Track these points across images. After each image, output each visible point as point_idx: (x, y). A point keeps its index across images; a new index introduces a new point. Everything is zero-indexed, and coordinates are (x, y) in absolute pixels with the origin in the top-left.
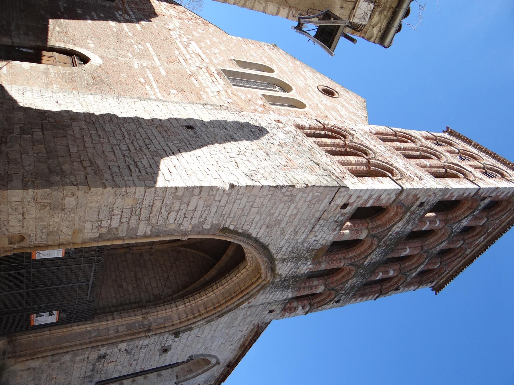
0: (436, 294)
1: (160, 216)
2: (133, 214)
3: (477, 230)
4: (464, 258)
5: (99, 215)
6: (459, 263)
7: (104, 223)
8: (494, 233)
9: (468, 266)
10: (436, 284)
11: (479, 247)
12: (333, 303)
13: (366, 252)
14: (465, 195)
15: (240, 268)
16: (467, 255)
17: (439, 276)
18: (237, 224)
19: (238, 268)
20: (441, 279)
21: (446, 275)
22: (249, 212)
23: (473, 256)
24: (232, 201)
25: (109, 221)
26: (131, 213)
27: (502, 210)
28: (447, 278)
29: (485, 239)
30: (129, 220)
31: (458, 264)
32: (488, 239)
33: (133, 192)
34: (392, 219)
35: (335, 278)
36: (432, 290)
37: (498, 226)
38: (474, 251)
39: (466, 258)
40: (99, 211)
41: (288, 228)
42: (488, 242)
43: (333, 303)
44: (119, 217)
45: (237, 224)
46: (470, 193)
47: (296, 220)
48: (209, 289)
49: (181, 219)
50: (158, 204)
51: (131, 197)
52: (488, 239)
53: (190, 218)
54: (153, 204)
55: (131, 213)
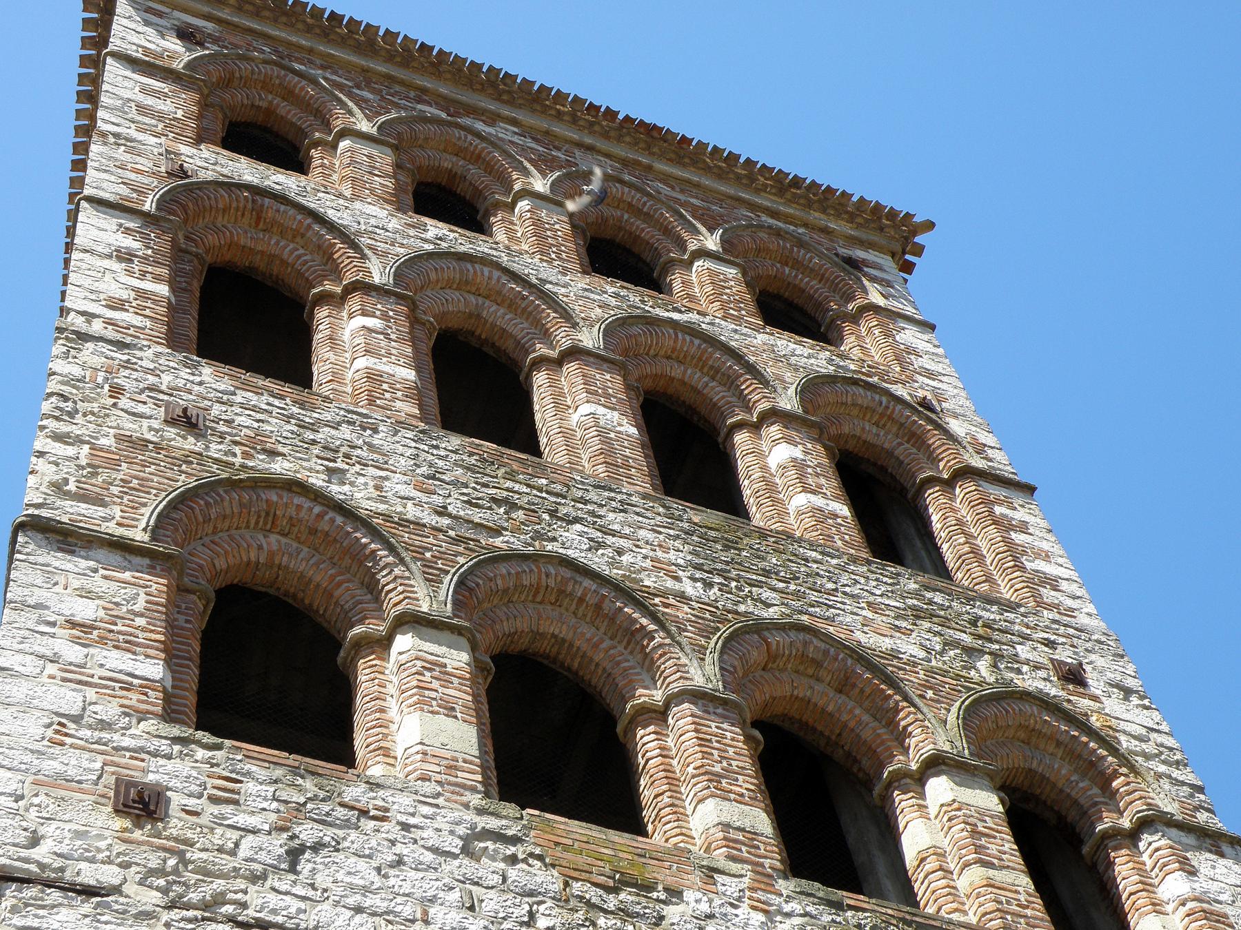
0: (930, 225)
4: (649, 168)
6: (689, 182)
8: (443, 90)
9: (685, 140)
11: (558, 129)
12: (1095, 698)
13: (598, 607)
17: (801, 244)
20: (825, 231)
21: (787, 219)
23: (619, 139)
27: (289, 95)
29: (492, 119)
31: (697, 186)
32: (492, 106)
34: (313, 531)
35: (867, 734)
36: (919, 250)
37: (397, 88)
38: (588, 140)
42: (511, 103)
43: (1095, 698)
46: (127, 231)
52: (492, 106)
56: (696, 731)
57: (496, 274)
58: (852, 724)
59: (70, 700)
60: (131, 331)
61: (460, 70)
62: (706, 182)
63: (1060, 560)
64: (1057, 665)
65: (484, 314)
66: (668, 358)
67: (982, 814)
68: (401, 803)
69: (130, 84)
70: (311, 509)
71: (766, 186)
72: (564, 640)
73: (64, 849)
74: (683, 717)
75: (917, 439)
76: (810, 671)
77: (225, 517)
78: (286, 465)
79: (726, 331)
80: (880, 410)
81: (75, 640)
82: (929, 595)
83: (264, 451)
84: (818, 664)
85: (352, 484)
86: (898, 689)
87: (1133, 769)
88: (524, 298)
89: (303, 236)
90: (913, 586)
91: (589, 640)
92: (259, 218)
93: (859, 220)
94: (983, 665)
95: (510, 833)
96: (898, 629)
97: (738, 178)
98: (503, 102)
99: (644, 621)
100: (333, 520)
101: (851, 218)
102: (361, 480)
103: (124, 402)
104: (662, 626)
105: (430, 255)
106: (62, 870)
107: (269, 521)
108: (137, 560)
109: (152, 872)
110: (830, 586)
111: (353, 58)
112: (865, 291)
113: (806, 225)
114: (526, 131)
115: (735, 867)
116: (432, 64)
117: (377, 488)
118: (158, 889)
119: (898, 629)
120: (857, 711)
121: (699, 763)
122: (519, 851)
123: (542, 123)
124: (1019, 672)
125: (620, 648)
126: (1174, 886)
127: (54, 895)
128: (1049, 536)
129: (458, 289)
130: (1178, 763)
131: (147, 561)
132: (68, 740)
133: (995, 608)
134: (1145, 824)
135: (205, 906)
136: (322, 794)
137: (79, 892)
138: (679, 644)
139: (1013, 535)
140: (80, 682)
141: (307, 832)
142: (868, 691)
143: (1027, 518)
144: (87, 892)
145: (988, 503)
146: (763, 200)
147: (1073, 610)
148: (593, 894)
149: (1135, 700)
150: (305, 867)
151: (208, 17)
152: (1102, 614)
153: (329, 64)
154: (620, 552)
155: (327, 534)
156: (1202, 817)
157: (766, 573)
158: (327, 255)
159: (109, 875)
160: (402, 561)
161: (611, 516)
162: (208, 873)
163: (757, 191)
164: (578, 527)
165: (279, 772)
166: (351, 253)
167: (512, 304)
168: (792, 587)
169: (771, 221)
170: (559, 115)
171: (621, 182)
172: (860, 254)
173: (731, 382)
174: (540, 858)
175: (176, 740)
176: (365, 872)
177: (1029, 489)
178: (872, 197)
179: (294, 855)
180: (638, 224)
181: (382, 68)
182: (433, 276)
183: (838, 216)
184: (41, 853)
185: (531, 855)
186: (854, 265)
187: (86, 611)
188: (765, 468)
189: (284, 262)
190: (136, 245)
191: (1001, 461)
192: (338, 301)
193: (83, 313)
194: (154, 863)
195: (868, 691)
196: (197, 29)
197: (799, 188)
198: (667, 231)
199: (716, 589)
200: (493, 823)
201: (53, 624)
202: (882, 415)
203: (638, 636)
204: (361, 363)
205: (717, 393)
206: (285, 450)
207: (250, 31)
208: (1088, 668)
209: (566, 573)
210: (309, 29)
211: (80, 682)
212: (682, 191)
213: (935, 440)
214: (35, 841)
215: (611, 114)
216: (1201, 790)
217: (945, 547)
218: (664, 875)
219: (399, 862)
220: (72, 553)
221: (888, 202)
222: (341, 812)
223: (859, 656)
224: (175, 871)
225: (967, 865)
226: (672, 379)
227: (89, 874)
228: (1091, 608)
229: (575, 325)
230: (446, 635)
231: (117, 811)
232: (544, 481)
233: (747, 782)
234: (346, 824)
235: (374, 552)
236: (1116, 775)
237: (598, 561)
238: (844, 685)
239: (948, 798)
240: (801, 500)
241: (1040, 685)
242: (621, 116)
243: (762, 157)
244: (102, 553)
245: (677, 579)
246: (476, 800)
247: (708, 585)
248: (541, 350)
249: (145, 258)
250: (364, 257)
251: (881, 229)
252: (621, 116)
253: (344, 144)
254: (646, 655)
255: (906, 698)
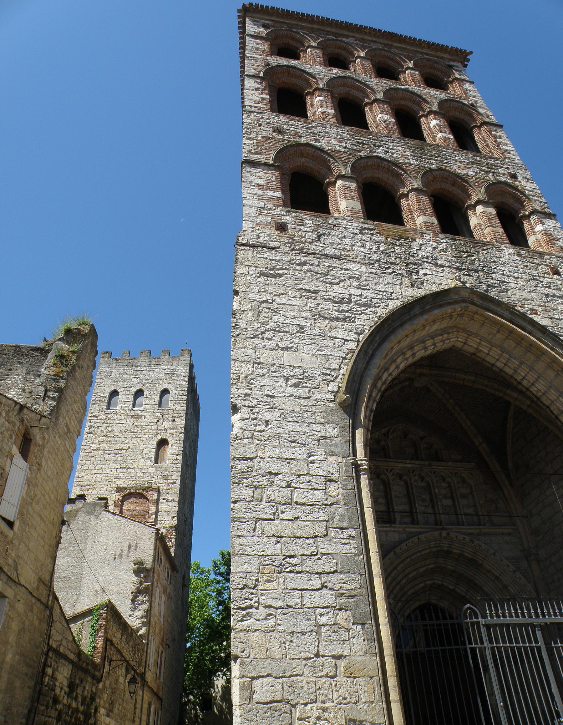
0: (471, 53)
1: (306, 519)
2: (299, 569)
3: (336, 52)
4: (392, 45)
5: (303, 634)
6: (403, 48)
7: (323, 620)
9: (401, 36)
10: (454, 61)
13: (388, 169)
14: (258, 86)
15: (472, 350)
16: (385, 45)
17: (435, 62)
18: (325, 380)
19: (474, 354)
20: (442, 58)
22: (294, 367)
24: (269, 399)
25: (319, 611)
26: (298, 572)
27: (293, 38)
28: (437, 50)
29: (347, 37)
30: (317, 573)
31: (405, 49)
32: (347, 33)
33: (243, 575)
34: (313, 156)
37: (321, 32)
38: (374, 39)
39: (390, 43)
40: (293, 633)
41: (334, 294)
42: (352, 31)
43: (520, 182)
44: (306, 594)
45: (325, 380)
47: (313, 288)
48: (535, 393)
49: (314, 479)
50: (276, 527)
51: (255, 578)
52: (347, 33)
53: (310, 465)
54: (273, 536)
55: (298, 572)
56: (416, 199)
57: (353, 81)
58: (456, 194)
59: (261, 204)
60: (261, 109)
61: (337, 24)
62: (408, 47)
63: (510, 145)
64: (510, 174)
65: (351, 92)
66: (401, 99)
67: (490, 214)
68: (343, 222)
69: (252, 42)
70: (312, 150)
71: (424, 46)
72: (380, 178)
73: (265, 239)
74: (412, 196)
75: (471, 115)
76: (445, 181)
77: (291, 155)
78: (304, 139)
79: (416, 90)
80: (460, 108)
81: (260, 189)
82: (475, 158)
83: (298, 136)
84: (447, 179)
85: (321, 142)
86: (468, 184)
87: (529, 199)
88: (361, 87)
89: (301, 77)
90: (471, 156)
91: (386, 178)
92: (289, 74)
93: (451, 53)
94: (490, 175)
95: (371, 228)
96: (467, 168)
97: (417, 45)
98: (350, 32)
99: (401, 171)
100: (318, 153)
101: (449, 53)
102: (324, 141)
103: (263, 128)
104: (405, 172)
105: (334, 78)
106: (266, 244)
107: (302, 154)
108: (271, 168)
109: (286, 243)
110: (449, 158)
111: (309, 25)
112: (454, 74)
113: (436, 57)
114: (357, 39)
115: (428, 232)
116: (330, 23)
117: (328, 143)
118: (288, 247)
119: (467, 168)
120: (458, 190)
121: (417, 207)
122: (374, 232)
123: (361, 36)
124: (500, 176)
125: (395, 179)
126: (539, 228)
127: (265, 250)
128: (507, 139)
129: (343, 86)
130: (541, 196)
131: (273, 168)
132: (262, 213)
133: (493, 160)
134: (532, 213)
135: (299, 250)
136: (324, 222)
137: (271, 249)
138: (410, 176)
139: (497, 140)
140: (263, 199)
141: (321, 231)
142: (460, 185)
143: (501, 134)
144: (273, 248)
145: (491, 131)
146: (424, 51)
147: (514, 159)
148: (393, 241)
149: (530, 181)
150: (322, 239)
151: (270, 20)
152: (521, 159)
153: (302, 28)
154: (393, 154)
155: (317, 156)
156: (546, 210)
157: (432, 156)
158: (307, 81)
159: (277, 244)
160: (337, 161)
161: (390, 144)
162: (299, 242)
163: (422, 48)
164: (381, 148)
165: (313, 217)
166: (314, 80)
167: (358, 89)
168: (439, 159)
169: (427, 57)
170: (366, 33)
171: (384, 50)
172: (452, 63)
173: (419, 104)
174: (379, 233)
175: (287, 211)
176: (337, 240)
177: (501, 126)
178: (455, 46)
179: (319, 237)
180: (390, 62)
181: (316, 27)
182: (336, 83)
183: (445, 53)
184: (261, 240)
185: (377, 233)
186: (451, 67)
187: (261, 182)
188: (430, 127)
189: (297, 85)
190: (259, 86)
191: (493, 119)
192: (311, 94)
193: (249, 106)
194: (286, 241)
195: (460, 185)
196: (267, 24)
197: (434, 46)
198: (398, 63)
199: (419, 161)
200: (366, 226)
201: (254, 186)
202: (461, 109)
203: (399, 176)
204: (320, 110)
205: (416, 108)
206: (304, 135)
207: (280, 22)
208: (518, 174)
209: (379, 161)
210: (296, 19)
211: (263, 199)
212: (401, 51)
213: (475, 115)
214: (259, 237)
215: (380, 31)
216: (546, 203)
217: (479, 144)
218: (411, 235)
219: (345, 237)
220: (256, 168)
221: (459, 47)
222: (329, 226)
223: (458, 176)
224: (292, 242)
225: (487, 227)
226: (403, 105)
227: (272, 244)
228: (518, 158)
229: (375, 93)
230: (350, 180)
231: (276, 229)
232: (371, 137)
233: (430, 211)
234: (331, 229)
235: (329, 160)
236: (525, 201)
237: (387, 157)
238: (454, 184)
239: (482, 210)
240: (440, 135)
241: (505, 179)
242: (383, 31)
243: (423, 38)
244: (263, 167)
245: (409, 159)
246: (362, 220)
247: (417, 160)
248: (367, 101)
249: (262, 89)
250: (317, 81)
251: (458, 55)
252: (383, 31)
253: (309, 50)
254: (402, 180)
255: (470, 186)
